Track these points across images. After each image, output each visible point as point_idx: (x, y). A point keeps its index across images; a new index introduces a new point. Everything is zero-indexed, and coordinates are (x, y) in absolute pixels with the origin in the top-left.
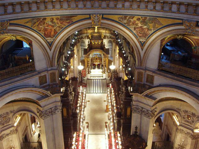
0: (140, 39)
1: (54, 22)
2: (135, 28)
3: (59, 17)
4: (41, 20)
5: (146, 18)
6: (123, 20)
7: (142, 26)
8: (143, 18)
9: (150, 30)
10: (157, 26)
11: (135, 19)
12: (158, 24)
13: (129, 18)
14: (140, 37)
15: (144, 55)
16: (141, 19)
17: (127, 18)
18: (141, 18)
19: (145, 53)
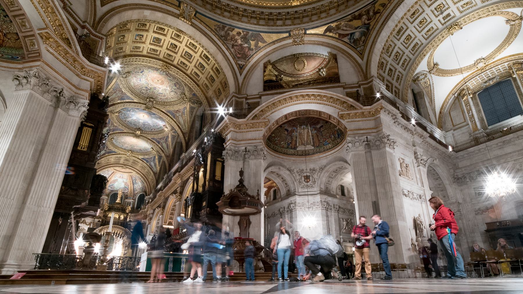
15: (243, 80)
19: (245, 78)
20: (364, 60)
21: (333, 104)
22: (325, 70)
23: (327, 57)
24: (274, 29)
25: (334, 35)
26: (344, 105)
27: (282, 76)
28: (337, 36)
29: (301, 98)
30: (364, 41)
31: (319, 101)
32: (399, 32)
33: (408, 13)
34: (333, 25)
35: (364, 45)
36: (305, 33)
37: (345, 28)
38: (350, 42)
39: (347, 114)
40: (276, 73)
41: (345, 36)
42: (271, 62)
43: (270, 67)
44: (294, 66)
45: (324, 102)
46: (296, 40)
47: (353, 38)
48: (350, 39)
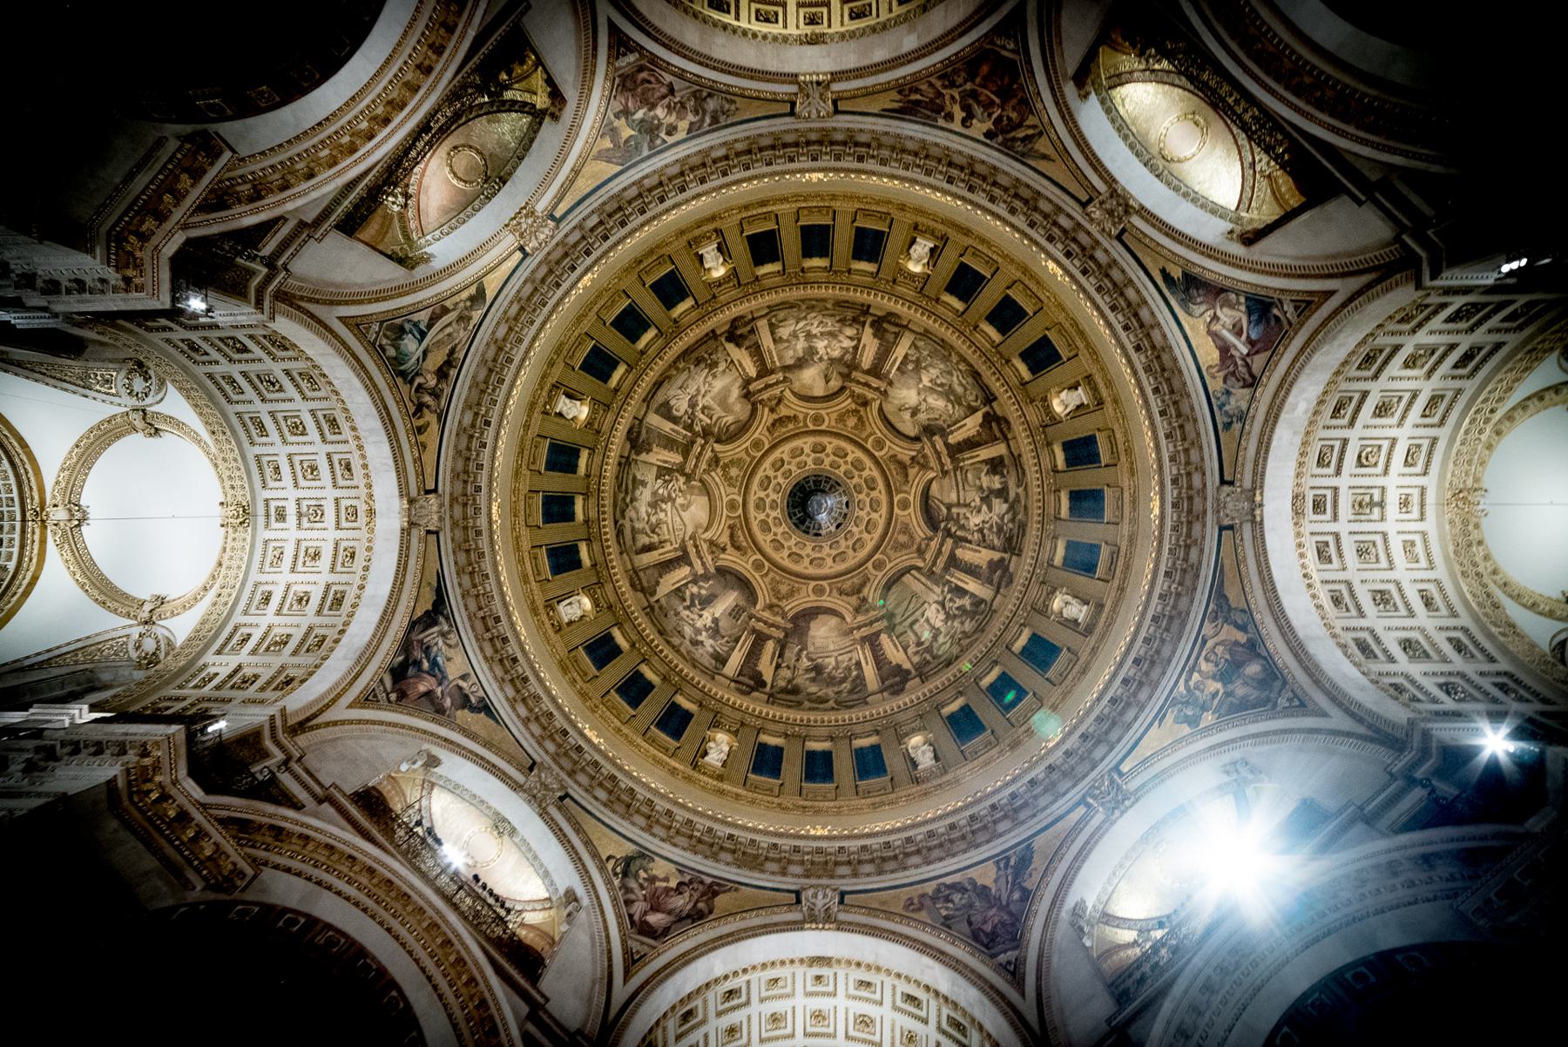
0: (637, 60)
1: (963, 109)
2: (672, 91)
3: (941, 122)
4: (1000, 138)
5: (650, 148)
6: (722, 107)
7: (652, 113)
8: (658, 142)
9: (621, 112)
10: (607, 143)
11: (683, 125)
12: (608, 150)
13: (702, 120)
14: (641, 69)
16: (663, 135)
17: (708, 120)
18: (665, 137)
20: (337, 321)
21: (283, 156)
22: (396, 208)
23: (423, 241)
24: (595, 202)
25: (456, 298)
26: (248, 186)
27: (486, 99)
28: (448, 304)
29: (395, 95)
30: (384, 350)
31: (333, 129)
32: (333, 423)
33: (361, 462)
34: (477, 315)
35: (373, 344)
36: (522, 249)
37: (449, 330)
38: (409, 321)
39: (205, 172)
40: (508, 95)
41: (431, 319)
42: (547, 119)
43: (541, 101)
44: (478, 152)
45: (315, 140)
46: (530, 221)
47: (411, 332)
48: (416, 325)
